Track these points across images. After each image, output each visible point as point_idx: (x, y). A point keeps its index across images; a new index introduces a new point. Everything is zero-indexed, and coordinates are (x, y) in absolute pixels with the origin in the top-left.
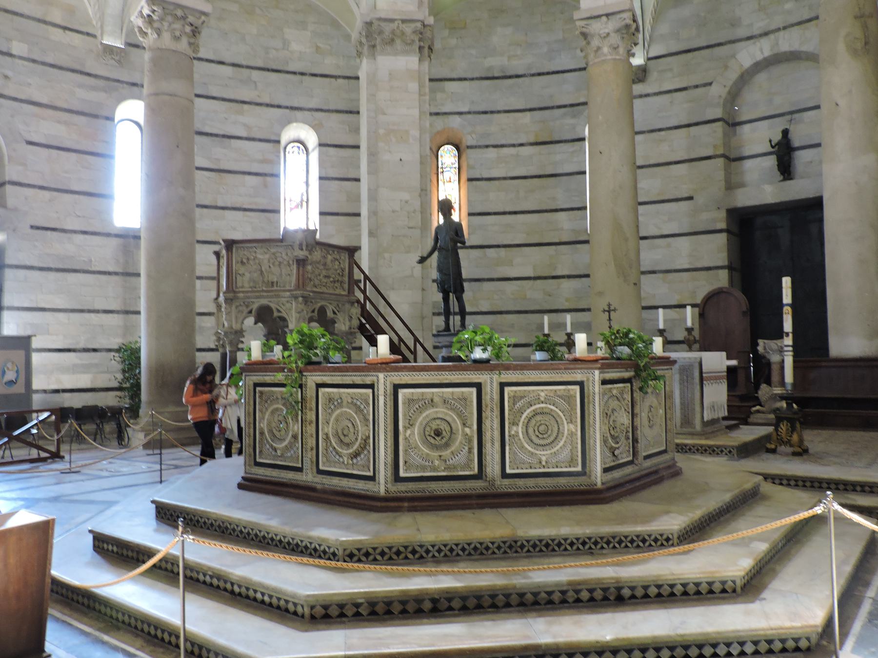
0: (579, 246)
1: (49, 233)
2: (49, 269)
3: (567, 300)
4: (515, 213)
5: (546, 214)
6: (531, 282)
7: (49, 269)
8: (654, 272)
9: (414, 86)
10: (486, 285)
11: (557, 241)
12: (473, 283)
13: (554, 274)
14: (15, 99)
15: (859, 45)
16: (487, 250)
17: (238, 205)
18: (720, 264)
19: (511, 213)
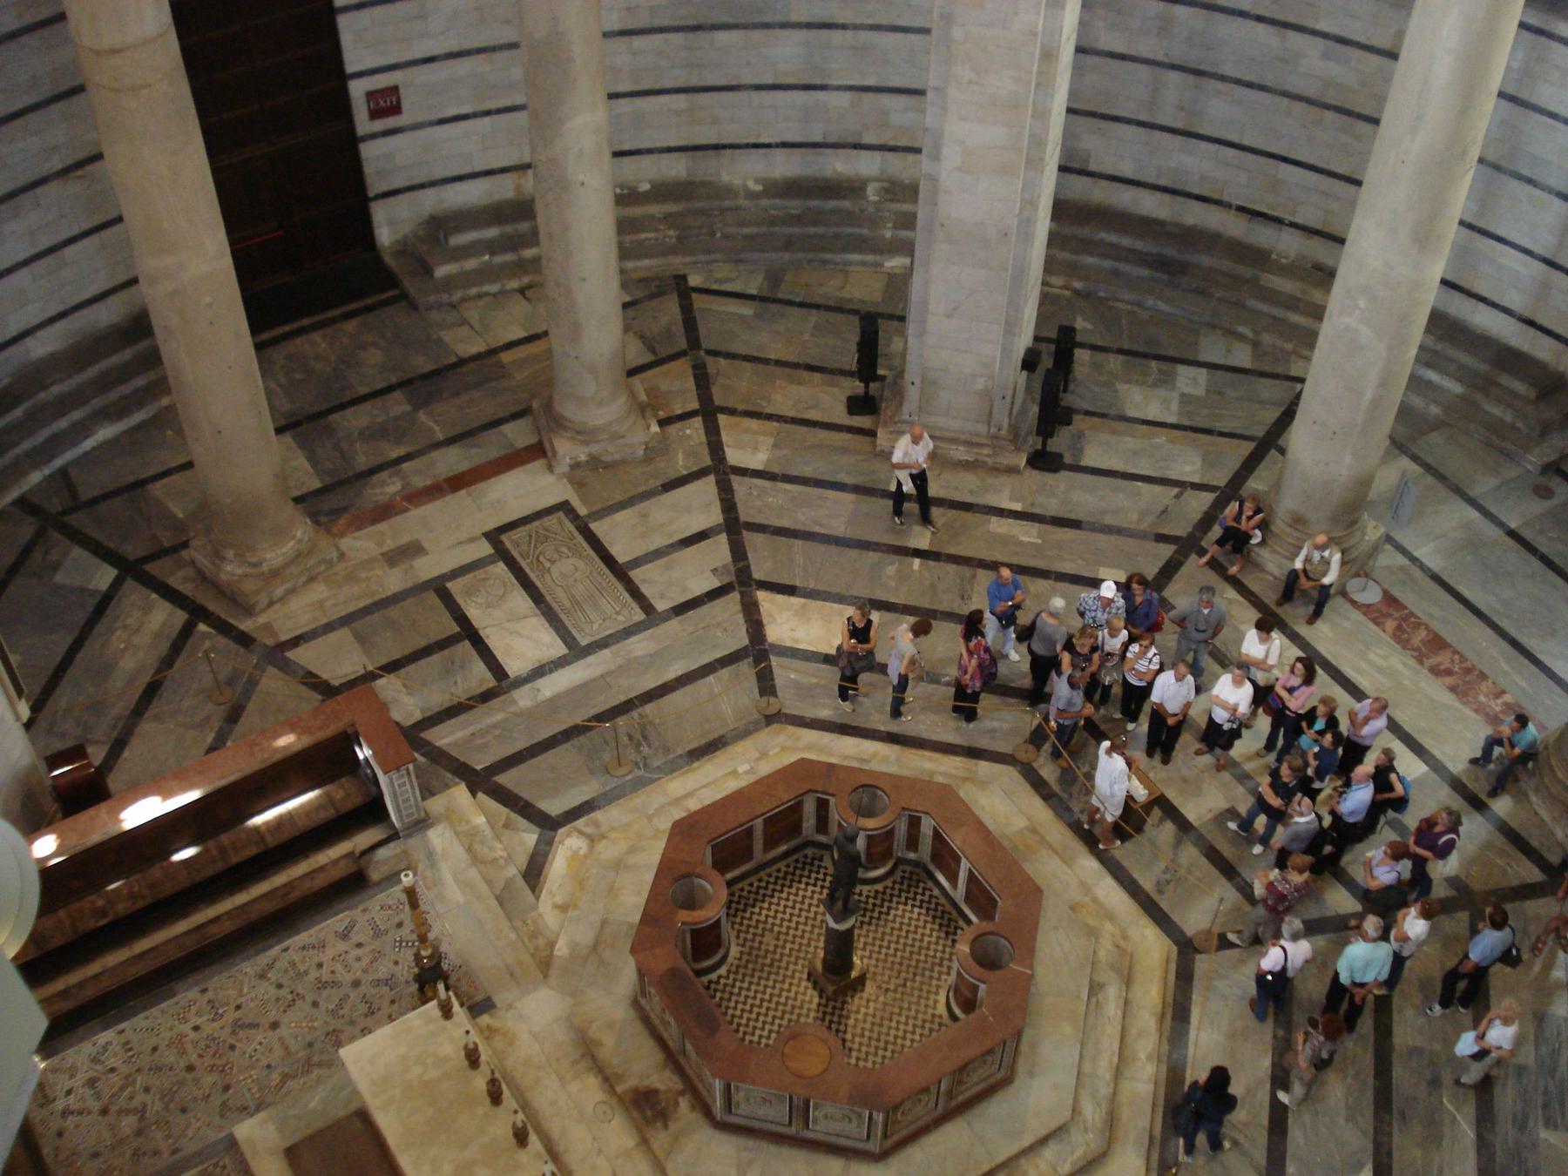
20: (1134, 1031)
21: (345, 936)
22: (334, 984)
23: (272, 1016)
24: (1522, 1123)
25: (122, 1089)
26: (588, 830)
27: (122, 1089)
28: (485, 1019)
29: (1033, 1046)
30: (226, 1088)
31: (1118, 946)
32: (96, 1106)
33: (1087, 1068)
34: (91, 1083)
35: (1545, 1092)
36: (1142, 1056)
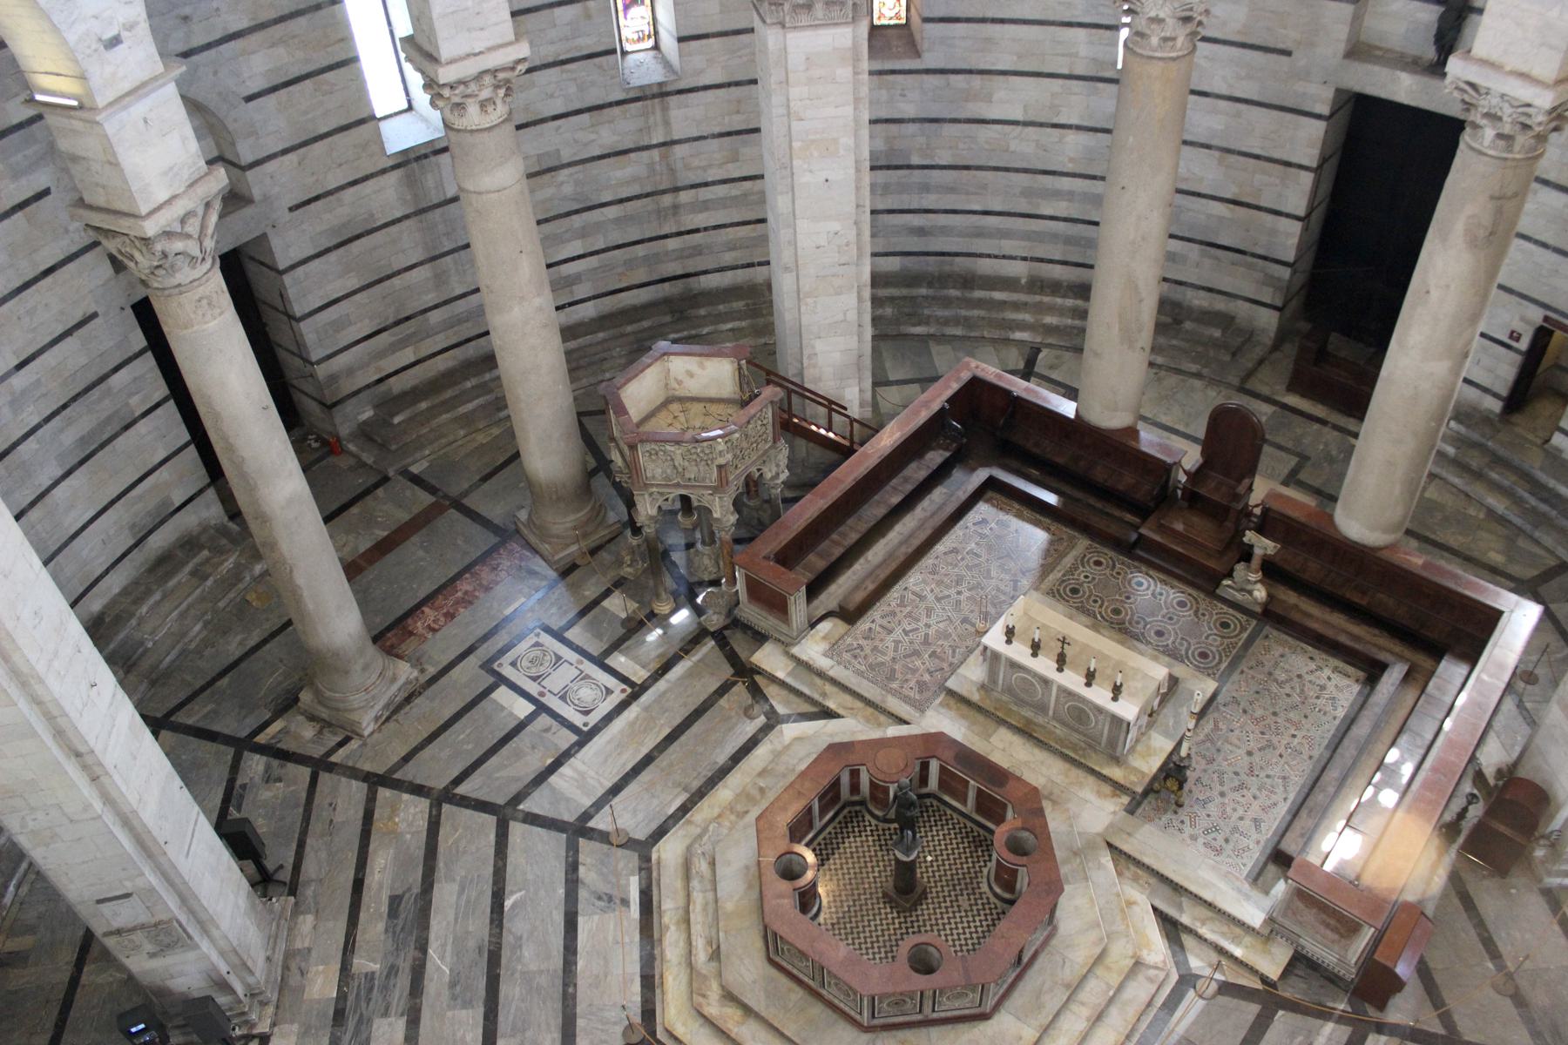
0: (1100, 85)
1: (313, 206)
2: (327, 251)
3: (1071, 160)
4: (1002, 21)
5: (1052, 28)
6: (1019, 128)
7: (327, 251)
8: (1208, 147)
9: (844, 73)
10: (949, 129)
11: (1066, 71)
12: (927, 125)
13: (1055, 121)
14: (209, 46)
15: (1482, 233)
16: (953, 77)
17: (551, 60)
18: (1306, 162)
19: (994, 21)
20: (682, 944)
21: (1257, 822)
22: (1236, 789)
23: (1257, 758)
24: (392, 971)
25: (1302, 691)
26: (1152, 972)
27: (1302, 691)
28: (1126, 800)
29: (750, 887)
30: (1245, 711)
31: (704, 996)
32: (1308, 678)
33: (710, 895)
34: (1323, 688)
35: (369, 1000)
36: (673, 928)
